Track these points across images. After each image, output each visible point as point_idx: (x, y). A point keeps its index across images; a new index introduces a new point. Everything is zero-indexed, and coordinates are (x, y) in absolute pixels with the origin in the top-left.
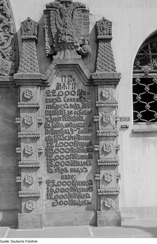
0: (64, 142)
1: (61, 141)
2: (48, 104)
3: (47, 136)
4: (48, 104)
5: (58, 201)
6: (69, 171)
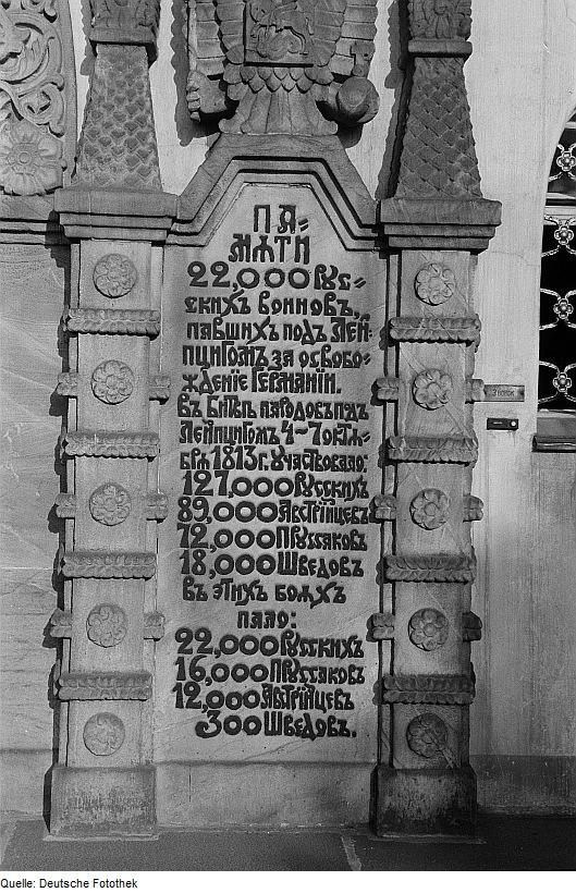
0: (253, 475)
2: (195, 318)
3: (187, 447)
4: (195, 318)
5: (221, 718)
6: (271, 594)
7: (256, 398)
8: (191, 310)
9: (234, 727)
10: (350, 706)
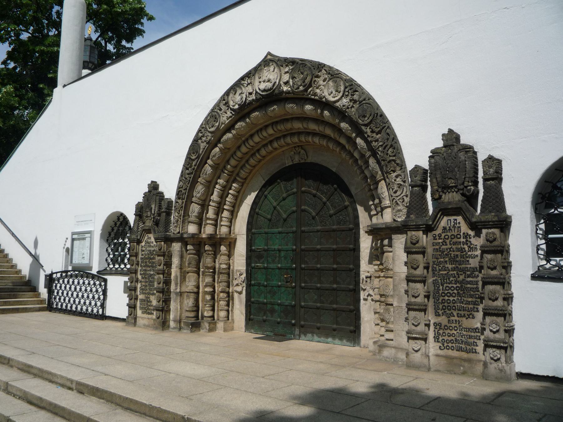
0: (450, 286)
1: (448, 285)
2: (435, 247)
3: (434, 279)
4: (435, 247)
5: (445, 345)
7: (450, 266)
8: (433, 246)
9: (447, 348)
10: (477, 346)
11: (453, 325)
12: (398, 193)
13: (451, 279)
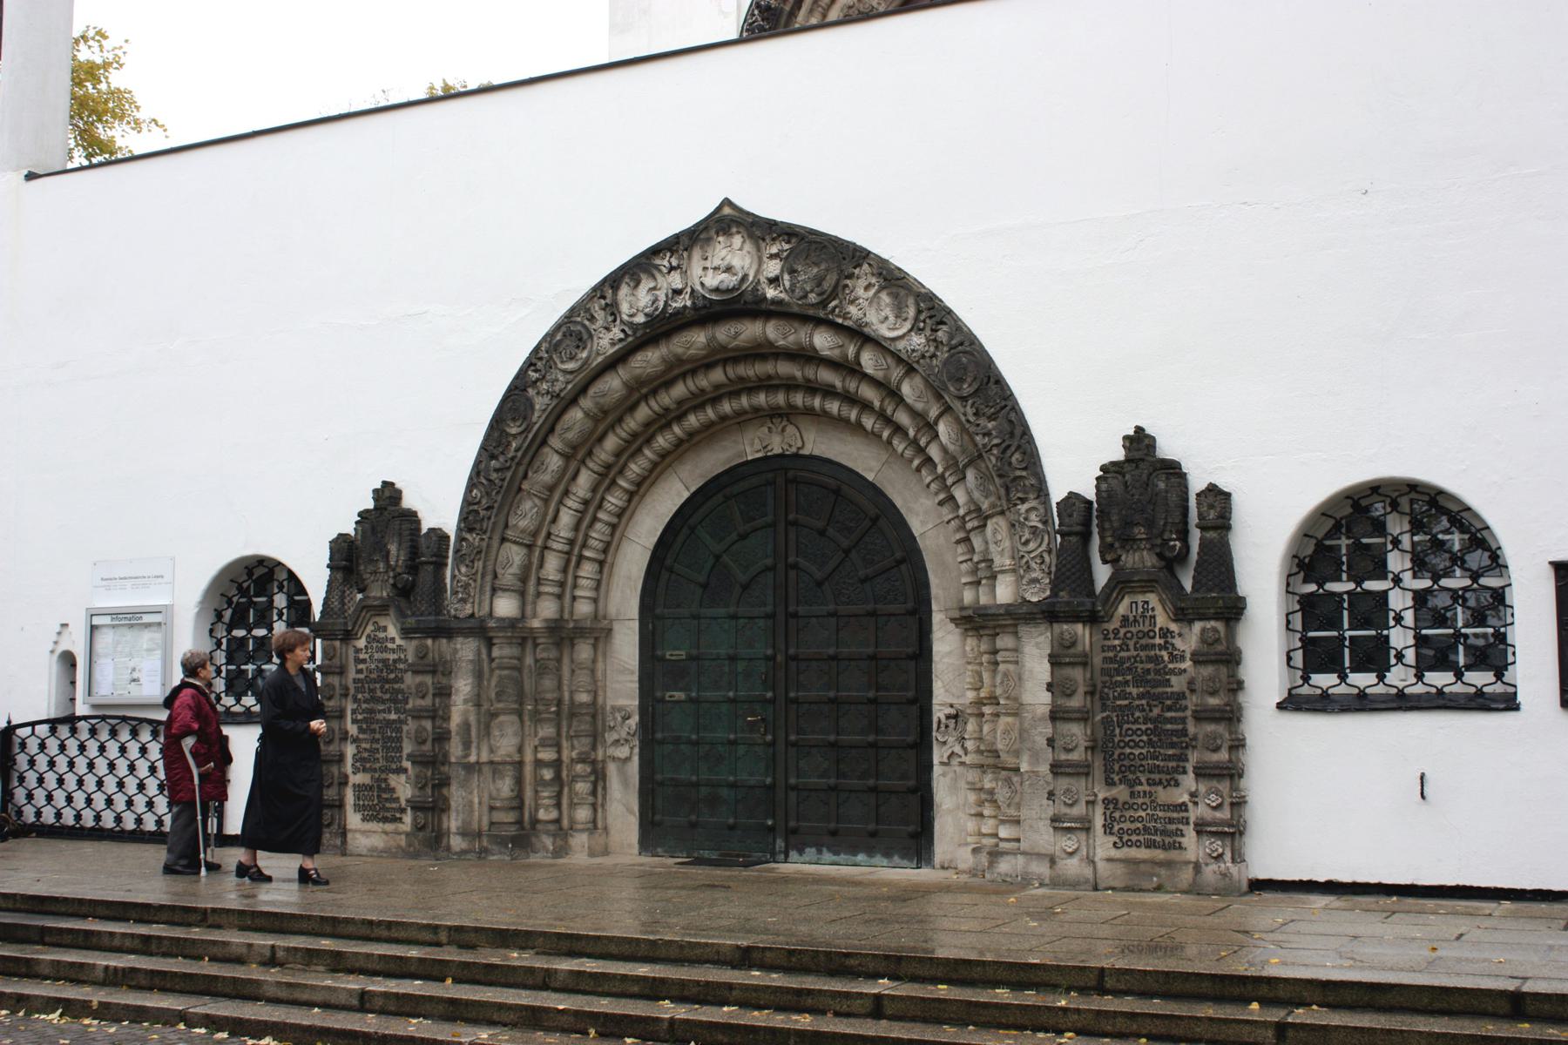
0: (1134, 727)
7: (1135, 691)
11: (1140, 801)
12: (1032, 546)
13: (1137, 714)
